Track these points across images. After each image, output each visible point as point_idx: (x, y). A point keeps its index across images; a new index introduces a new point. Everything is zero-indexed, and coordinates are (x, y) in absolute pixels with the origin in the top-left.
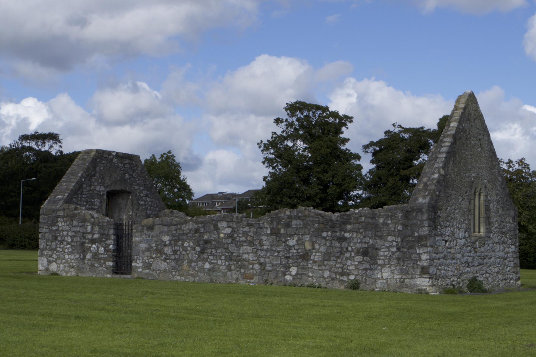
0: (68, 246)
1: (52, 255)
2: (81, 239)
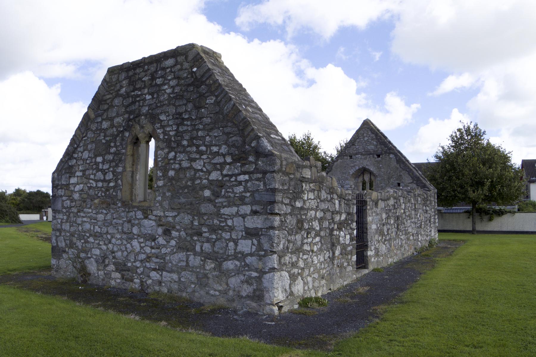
0: (318, 239)
1: (297, 262)
2: (330, 223)
